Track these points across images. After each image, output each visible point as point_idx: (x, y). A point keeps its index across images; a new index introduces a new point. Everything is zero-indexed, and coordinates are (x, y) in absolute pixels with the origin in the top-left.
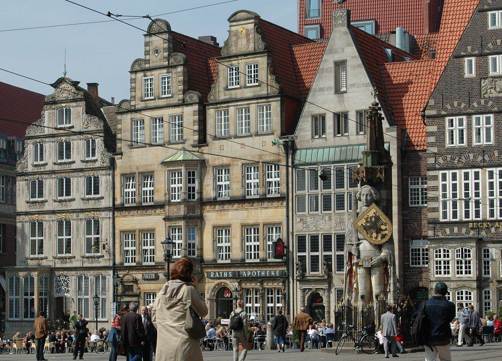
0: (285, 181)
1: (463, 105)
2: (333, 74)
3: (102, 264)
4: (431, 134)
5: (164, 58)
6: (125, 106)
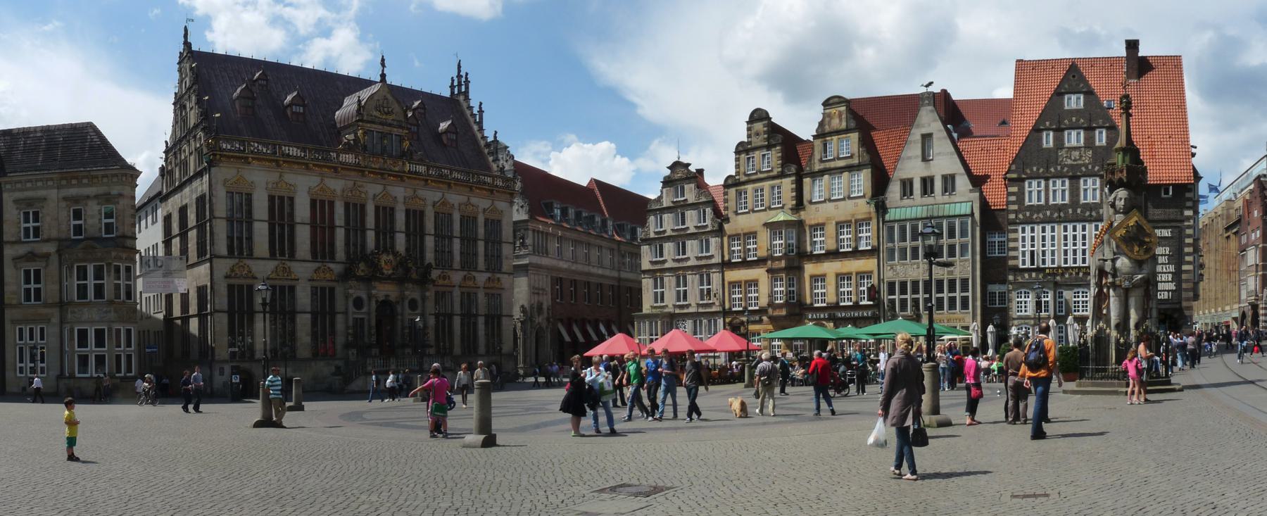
0: (876, 236)
2: (920, 145)
3: (714, 309)
5: (764, 139)
6: (730, 182)
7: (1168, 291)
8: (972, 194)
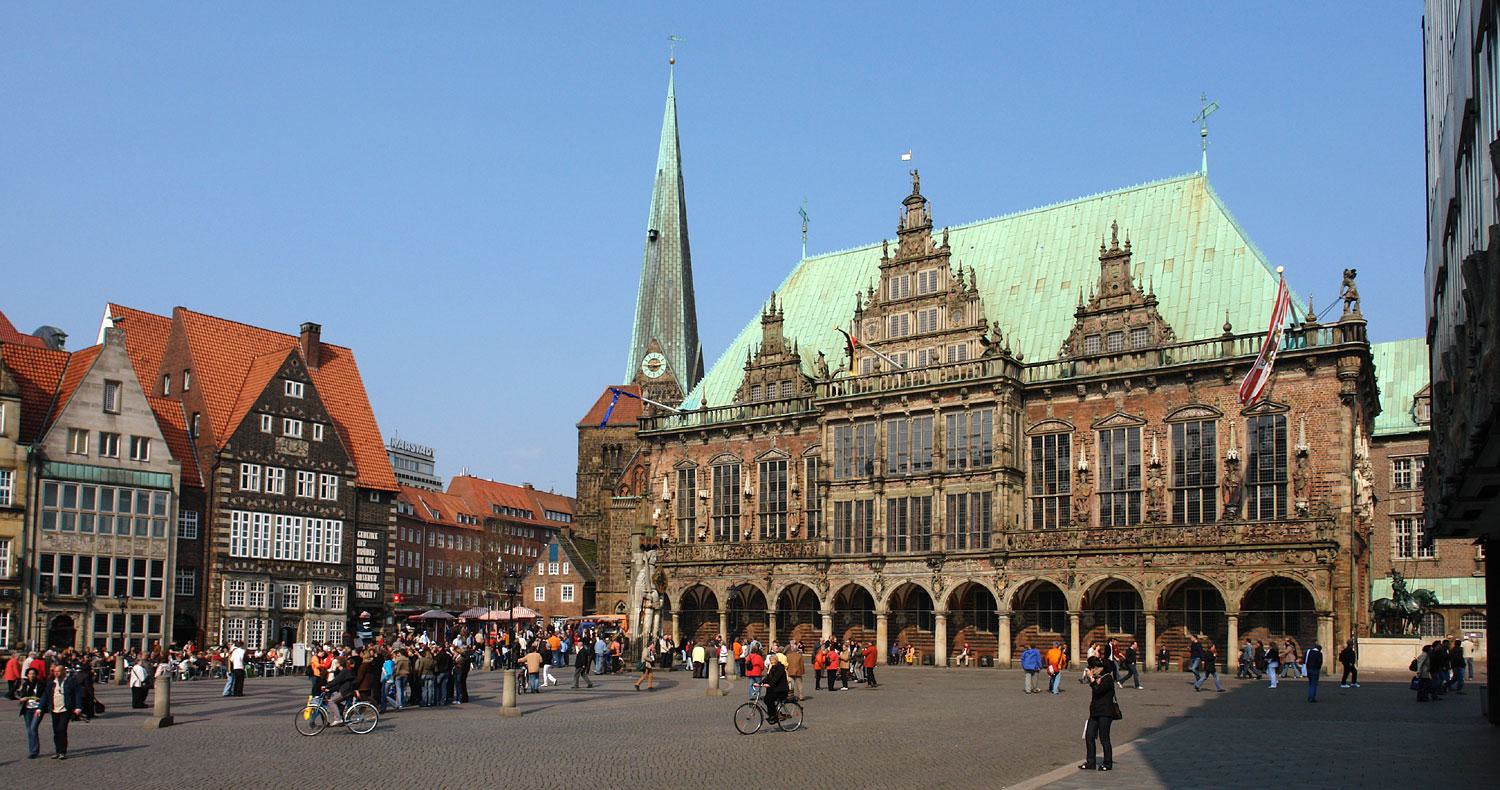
1: (258, 456)
4: (227, 475)
7: (373, 591)
8: (172, 466)
